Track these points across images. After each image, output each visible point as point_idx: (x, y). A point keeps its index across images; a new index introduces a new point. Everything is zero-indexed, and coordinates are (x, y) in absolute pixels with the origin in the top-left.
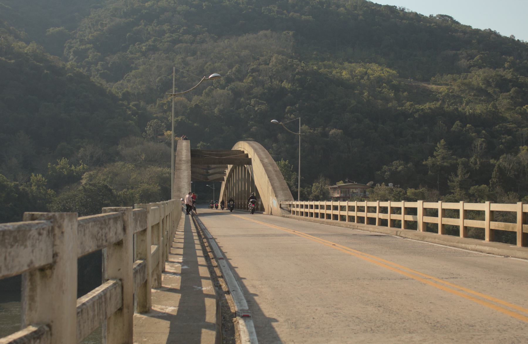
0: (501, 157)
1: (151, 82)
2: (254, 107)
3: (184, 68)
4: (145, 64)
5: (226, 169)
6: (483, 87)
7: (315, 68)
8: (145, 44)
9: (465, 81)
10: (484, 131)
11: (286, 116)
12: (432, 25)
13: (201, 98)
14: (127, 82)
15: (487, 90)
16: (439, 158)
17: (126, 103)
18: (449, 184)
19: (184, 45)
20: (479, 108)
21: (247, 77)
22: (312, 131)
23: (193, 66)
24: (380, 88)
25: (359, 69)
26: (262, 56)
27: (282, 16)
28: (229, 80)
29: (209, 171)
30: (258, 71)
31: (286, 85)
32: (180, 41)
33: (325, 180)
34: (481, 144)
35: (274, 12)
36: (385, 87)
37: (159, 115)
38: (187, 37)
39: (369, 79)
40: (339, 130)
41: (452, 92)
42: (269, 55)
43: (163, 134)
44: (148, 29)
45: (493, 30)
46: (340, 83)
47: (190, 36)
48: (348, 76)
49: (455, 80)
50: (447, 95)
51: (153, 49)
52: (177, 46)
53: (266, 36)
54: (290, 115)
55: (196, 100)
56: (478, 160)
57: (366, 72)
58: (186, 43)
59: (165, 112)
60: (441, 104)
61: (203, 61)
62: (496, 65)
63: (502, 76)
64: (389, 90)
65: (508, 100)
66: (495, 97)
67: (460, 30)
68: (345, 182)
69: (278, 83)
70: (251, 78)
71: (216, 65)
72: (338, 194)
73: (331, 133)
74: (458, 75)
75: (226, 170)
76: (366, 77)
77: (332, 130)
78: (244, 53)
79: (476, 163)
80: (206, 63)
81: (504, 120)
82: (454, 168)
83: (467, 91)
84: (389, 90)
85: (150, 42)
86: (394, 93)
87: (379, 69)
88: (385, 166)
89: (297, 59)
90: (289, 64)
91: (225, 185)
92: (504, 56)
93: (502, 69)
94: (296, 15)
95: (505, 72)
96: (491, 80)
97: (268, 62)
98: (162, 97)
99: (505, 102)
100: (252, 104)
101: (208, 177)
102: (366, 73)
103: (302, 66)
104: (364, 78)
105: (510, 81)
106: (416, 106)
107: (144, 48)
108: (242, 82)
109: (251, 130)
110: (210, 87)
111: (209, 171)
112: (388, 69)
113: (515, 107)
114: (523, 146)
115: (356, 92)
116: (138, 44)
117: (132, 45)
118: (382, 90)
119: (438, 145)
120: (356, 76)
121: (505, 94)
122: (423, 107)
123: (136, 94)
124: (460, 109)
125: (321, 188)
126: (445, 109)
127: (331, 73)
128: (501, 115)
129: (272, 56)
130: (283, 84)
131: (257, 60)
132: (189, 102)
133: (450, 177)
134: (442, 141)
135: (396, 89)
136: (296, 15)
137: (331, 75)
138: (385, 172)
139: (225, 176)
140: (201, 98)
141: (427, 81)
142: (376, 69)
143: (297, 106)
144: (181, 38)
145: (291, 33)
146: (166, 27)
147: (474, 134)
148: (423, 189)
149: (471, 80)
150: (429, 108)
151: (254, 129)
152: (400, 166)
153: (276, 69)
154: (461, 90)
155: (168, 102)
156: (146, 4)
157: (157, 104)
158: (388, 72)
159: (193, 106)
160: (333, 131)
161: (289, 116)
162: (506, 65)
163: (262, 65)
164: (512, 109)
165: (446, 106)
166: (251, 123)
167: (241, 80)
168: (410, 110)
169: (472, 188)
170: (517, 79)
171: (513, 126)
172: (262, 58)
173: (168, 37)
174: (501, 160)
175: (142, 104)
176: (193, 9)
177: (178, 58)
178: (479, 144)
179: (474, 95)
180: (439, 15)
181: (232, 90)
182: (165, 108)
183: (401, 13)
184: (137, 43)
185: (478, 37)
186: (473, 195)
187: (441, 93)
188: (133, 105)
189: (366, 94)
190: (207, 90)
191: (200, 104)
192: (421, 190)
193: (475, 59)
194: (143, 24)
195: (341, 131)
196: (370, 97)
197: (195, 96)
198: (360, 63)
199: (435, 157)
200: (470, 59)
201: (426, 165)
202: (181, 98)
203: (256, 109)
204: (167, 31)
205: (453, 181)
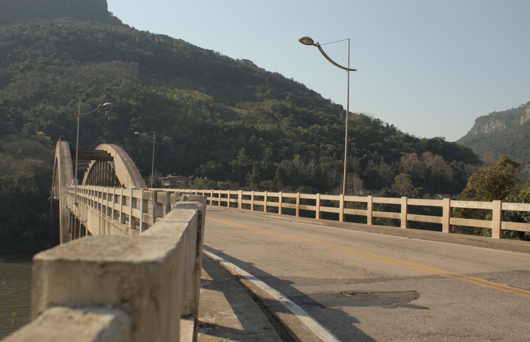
0: (282, 162)
1: (27, 93)
2: (107, 117)
3: (54, 84)
4: (22, 79)
6: (272, 112)
7: (154, 91)
8: (22, 64)
9: (260, 107)
10: (271, 143)
11: (131, 125)
12: (238, 66)
13: (66, 108)
14: (7, 92)
15: (274, 114)
16: (240, 161)
17: (6, 108)
18: (246, 179)
19: (54, 66)
20: (269, 127)
22: (150, 137)
23: (61, 83)
24: (200, 108)
25: (186, 94)
26: (114, 79)
28: (88, 96)
30: (111, 90)
31: (131, 101)
32: (51, 64)
33: (159, 173)
34: (269, 152)
35: (124, 47)
36: (204, 108)
37: (33, 119)
38: (57, 61)
39: (192, 101)
41: (250, 115)
43: (36, 134)
44: (25, 52)
45: (279, 73)
46: (172, 103)
47: (59, 60)
48: (177, 98)
49: (252, 106)
50: (247, 116)
51: (29, 68)
52: (48, 67)
53: (117, 64)
54: (134, 125)
55: (62, 109)
56: (266, 163)
57: (191, 96)
58: (56, 65)
59: (37, 116)
60: (242, 123)
61: (69, 80)
62: (281, 98)
63: (284, 106)
64: (207, 110)
65: (288, 123)
66: (279, 120)
67: (257, 71)
68: (173, 175)
69: (126, 100)
70: (105, 95)
71: (79, 83)
72: (168, 183)
73: (164, 139)
74: (255, 103)
76: (190, 100)
78: (101, 76)
79: (265, 165)
80: (71, 82)
81: (285, 136)
82: (250, 168)
83: (261, 115)
84: (207, 110)
85: (27, 62)
86: (210, 113)
87: (200, 95)
88: (202, 165)
89: (140, 83)
90: (135, 87)
92: (286, 92)
93: (284, 101)
94: (141, 51)
95: (286, 103)
96: (277, 108)
97: (119, 84)
98: (36, 105)
99: (286, 123)
100: (105, 115)
102: (190, 97)
103: (144, 89)
104: (189, 100)
105: (290, 109)
106: (225, 123)
107: (21, 66)
108: (99, 98)
109: (105, 134)
110: (74, 100)
112: (206, 96)
113: (293, 128)
114: (296, 155)
115: (183, 110)
116: (16, 63)
117: (12, 64)
118: (201, 110)
119: (240, 151)
120: (183, 99)
121: (286, 118)
122: (230, 124)
123: (14, 101)
124: (255, 127)
125: (156, 179)
126: (246, 126)
127: (165, 95)
128: (283, 132)
130: (129, 101)
132: (56, 111)
133: (247, 174)
134: (243, 149)
135: (212, 110)
136: (141, 51)
137: (165, 97)
138: (202, 169)
140: (66, 108)
141: (233, 105)
142: (198, 95)
143: (140, 118)
144: (52, 61)
145: (137, 64)
146: (40, 52)
147: (264, 145)
148: (228, 182)
149: (263, 107)
150: (234, 125)
151: (106, 133)
152: (212, 165)
153: (125, 90)
154: (256, 114)
155: (40, 109)
156: (24, 33)
157: (31, 110)
158: (206, 97)
159: (60, 113)
160: (165, 138)
161: (133, 125)
162: (287, 98)
163: (114, 86)
164: (290, 129)
165: (246, 124)
166: (104, 128)
167: (98, 96)
168: (221, 125)
169: (262, 182)
170: (294, 108)
171: (291, 140)
172: (114, 81)
173: (41, 60)
174: (282, 164)
175: (19, 109)
176: (62, 40)
177: (49, 76)
178: (267, 152)
179: (266, 118)
180: (243, 59)
181: (91, 103)
182: (38, 114)
183: (217, 56)
184: (16, 62)
185: (269, 77)
186: (262, 187)
187: (243, 115)
188: (13, 110)
189: (190, 112)
190: (71, 102)
191: (65, 113)
192: (227, 183)
193: (267, 92)
194: (21, 47)
195: (171, 138)
196: (193, 115)
197: (61, 106)
198: (186, 89)
199: (237, 160)
200: (263, 92)
201: (231, 165)
202: (51, 107)
203: (109, 118)
204: (41, 55)
205: (249, 177)
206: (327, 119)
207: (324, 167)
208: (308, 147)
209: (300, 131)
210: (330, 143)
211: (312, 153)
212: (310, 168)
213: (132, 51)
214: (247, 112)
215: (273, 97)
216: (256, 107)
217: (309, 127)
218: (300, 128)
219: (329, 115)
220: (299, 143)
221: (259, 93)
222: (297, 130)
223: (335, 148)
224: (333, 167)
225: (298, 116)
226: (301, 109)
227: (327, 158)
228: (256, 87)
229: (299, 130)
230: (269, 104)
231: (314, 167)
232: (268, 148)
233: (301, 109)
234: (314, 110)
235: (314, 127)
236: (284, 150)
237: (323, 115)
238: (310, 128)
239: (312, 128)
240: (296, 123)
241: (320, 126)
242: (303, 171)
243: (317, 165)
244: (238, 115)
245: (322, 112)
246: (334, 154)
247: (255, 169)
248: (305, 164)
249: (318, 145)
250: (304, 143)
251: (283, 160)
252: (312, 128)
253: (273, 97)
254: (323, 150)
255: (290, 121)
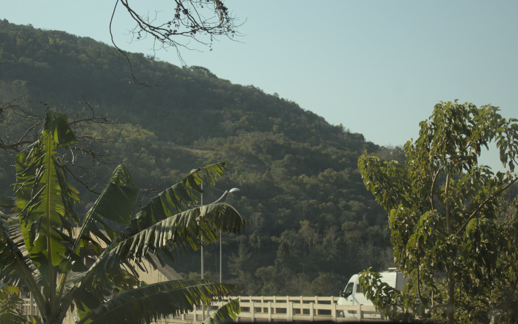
6: (253, 152)
10: (260, 204)
12: (189, 78)
34: (259, 219)
41: (219, 159)
45: (255, 86)
56: (258, 238)
63: (273, 141)
65: (282, 169)
66: (267, 164)
74: (223, 139)
79: (256, 242)
81: (280, 191)
92: (270, 118)
93: (271, 133)
95: (275, 136)
99: (279, 170)
113: (291, 176)
121: (278, 161)
124: (231, 179)
128: (276, 185)
133: (230, 257)
147: (250, 208)
149: (239, 145)
162: (275, 128)
170: (290, 144)
171: (291, 198)
174: (282, 237)
178: (256, 219)
180: (194, 66)
185: (240, 94)
193: (241, 120)
206: (344, 159)
207: (351, 238)
208: (321, 208)
209: (304, 181)
210: (355, 199)
211: (329, 217)
212: (328, 241)
214: (214, 155)
215: (252, 127)
216: (227, 145)
217: (317, 174)
218: (303, 177)
219: (346, 153)
220: (305, 201)
221: (228, 121)
222: (299, 179)
223: (365, 207)
224: (364, 239)
225: (297, 156)
226: (301, 145)
227: (354, 223)
228: (222, 112)
229: (303, 180)
230: (248, 140)
231: (335, 239)
232: (257, 213)
233: (301, 145)
234: (320, 146)
235: (325, 173)
236: (282, 214)
237: (337, 153)
238: (320, 176)
239: (323, 176)
240: (295, 169)
241: (335, 173)
242: (318, 247)
243: (339, 235)
244: (199, 160)
245: (335, 149)
246: (364, 217)
247: (244, 248)
248: (320, 235)
249: (336, 203)
250: (315, 200)
251: (284, 230)
252: (323, 176)
253: (252, 127)
254: (345, 212)
255: (286, 166)
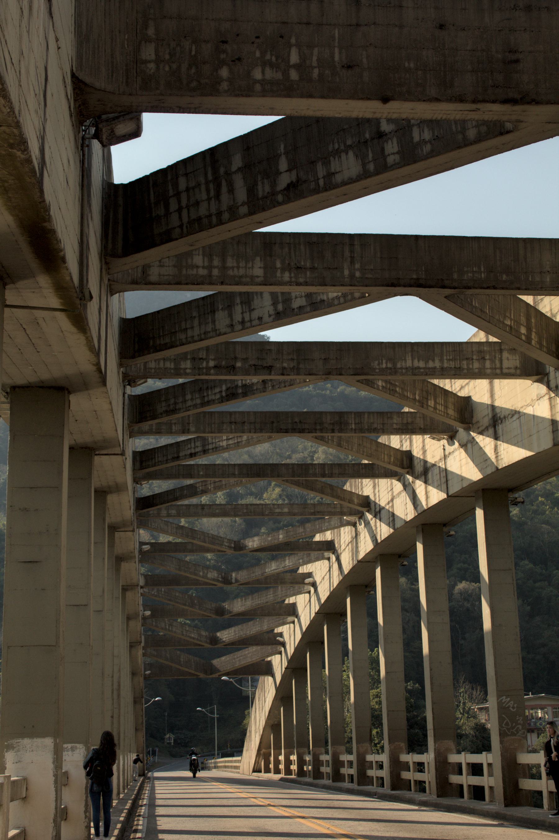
5: (290, 619)
21: (270, 489)
27: (324, 392)
29: (218, 634)
40: (474, 584)
42: (309, 450)
75: (284, 629)
77: (459, 584)
91: (277, 689)
101: (216, 662)
111: (218, 634)
129: (315, 452)
131: (287, 460)
139: (280, 653)
213: (328, 392)
